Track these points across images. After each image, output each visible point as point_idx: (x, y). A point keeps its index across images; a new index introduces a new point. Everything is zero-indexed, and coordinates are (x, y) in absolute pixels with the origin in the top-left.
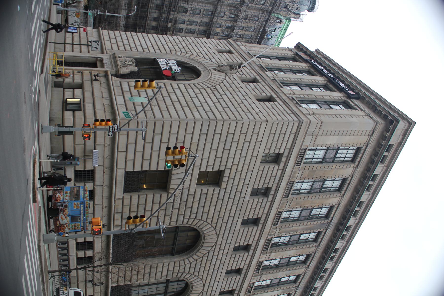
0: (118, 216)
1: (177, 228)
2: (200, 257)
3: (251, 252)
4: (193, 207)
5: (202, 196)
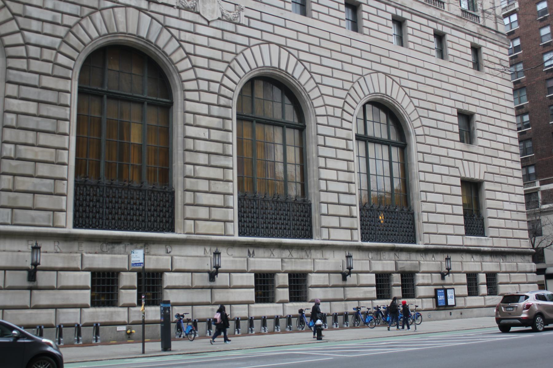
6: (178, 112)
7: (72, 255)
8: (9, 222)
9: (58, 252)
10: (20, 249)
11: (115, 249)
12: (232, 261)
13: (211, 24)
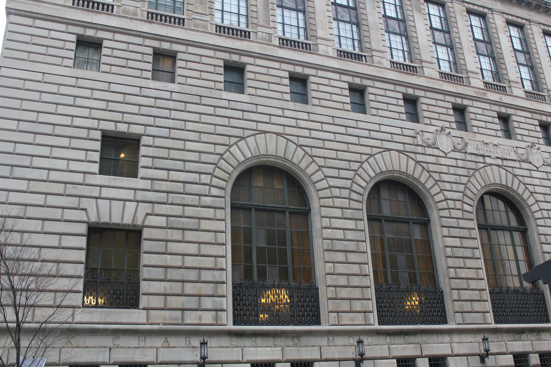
0: (191, 318)
1: (370, 219)
2: (526, 188)
3: (510, 111)
4: (182, 180)
5: (158, 166)
6: (534, 235)
13: (539, 169)
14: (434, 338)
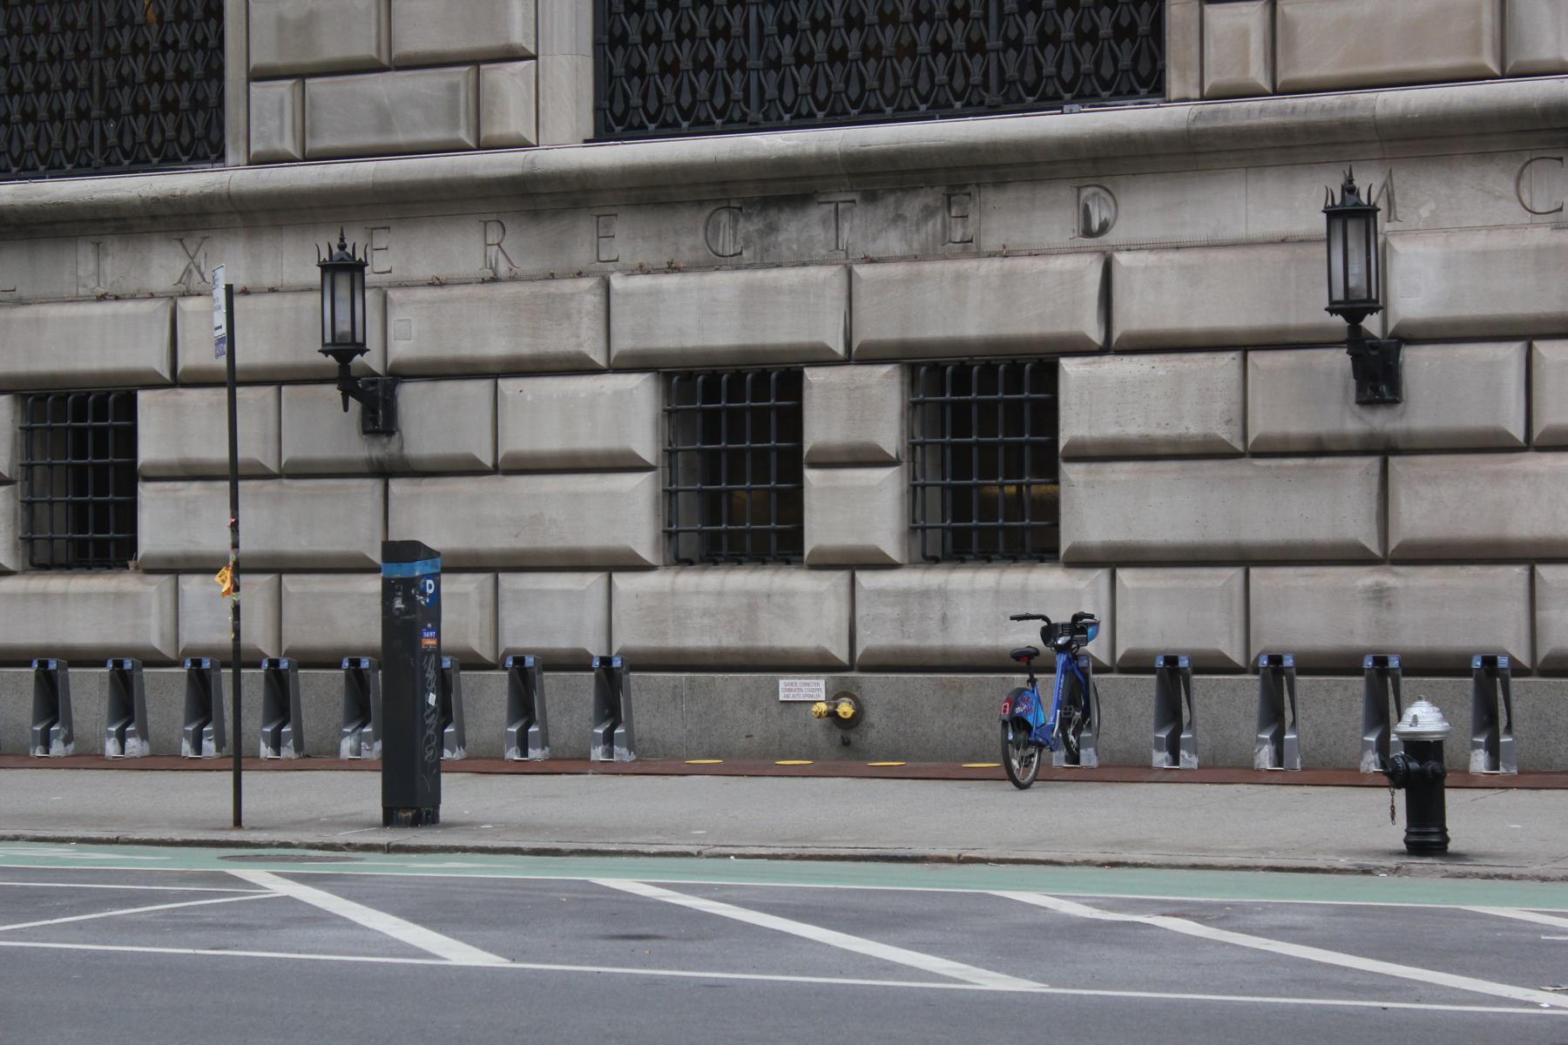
7: (553, 287)
8: (289, 146)
9: (495, 280)
10: (444, 272)
11: (782, 237)
12: (1539, 250)
14: (82, 265)
